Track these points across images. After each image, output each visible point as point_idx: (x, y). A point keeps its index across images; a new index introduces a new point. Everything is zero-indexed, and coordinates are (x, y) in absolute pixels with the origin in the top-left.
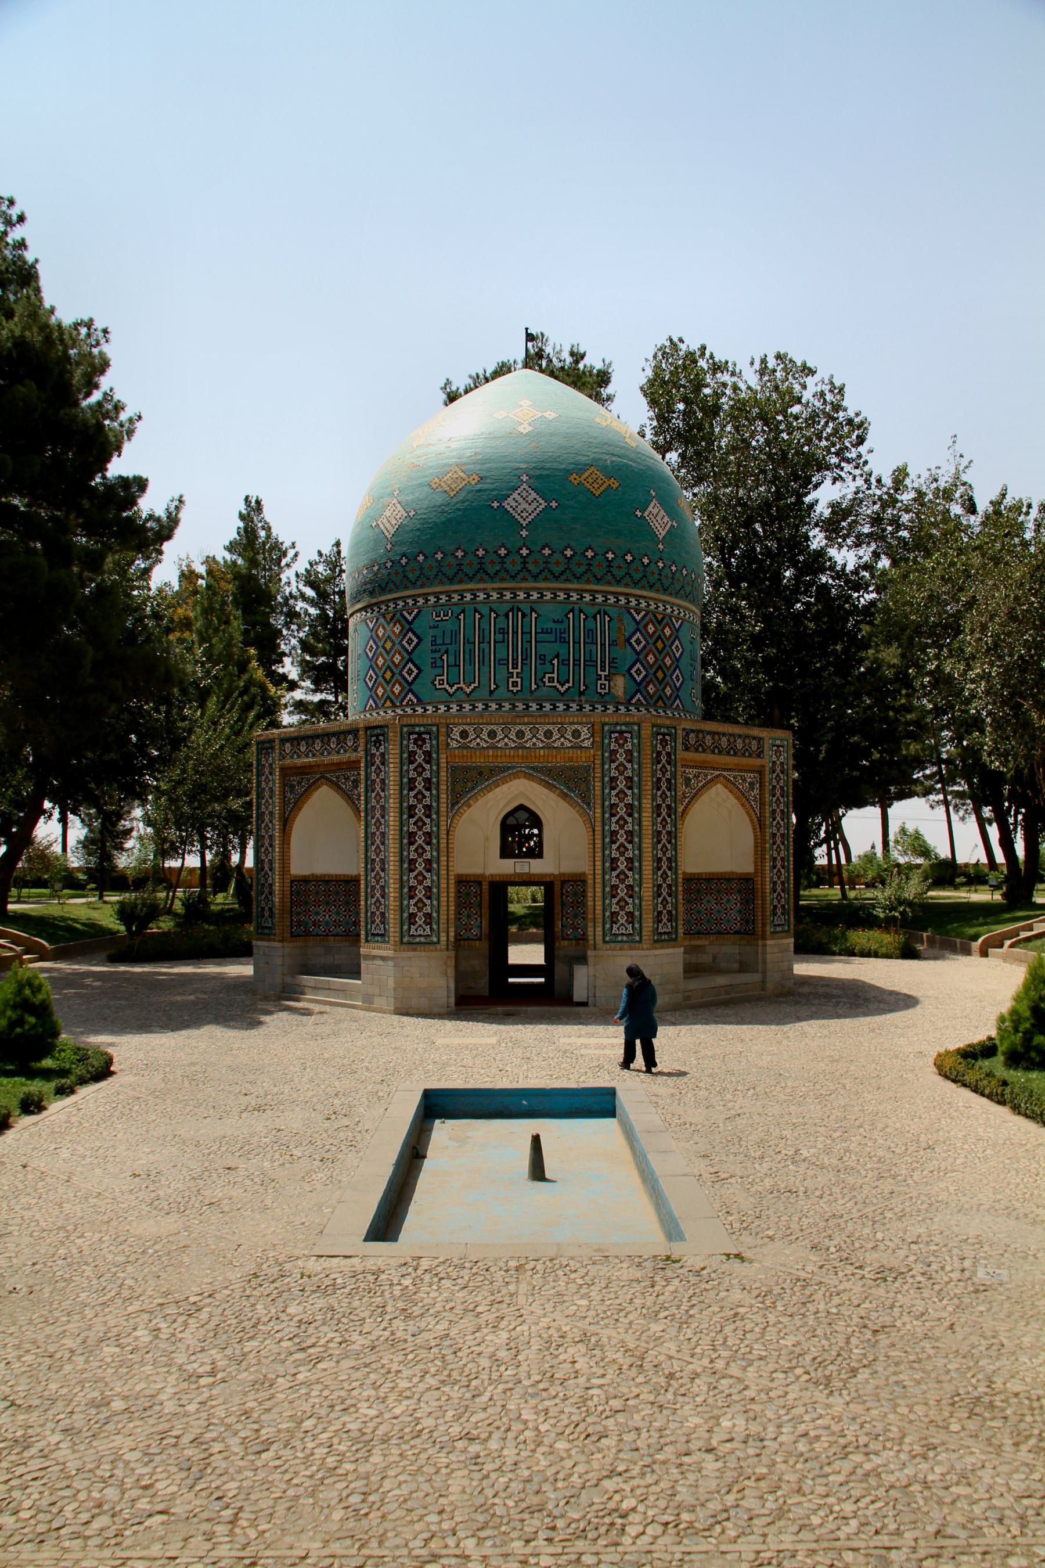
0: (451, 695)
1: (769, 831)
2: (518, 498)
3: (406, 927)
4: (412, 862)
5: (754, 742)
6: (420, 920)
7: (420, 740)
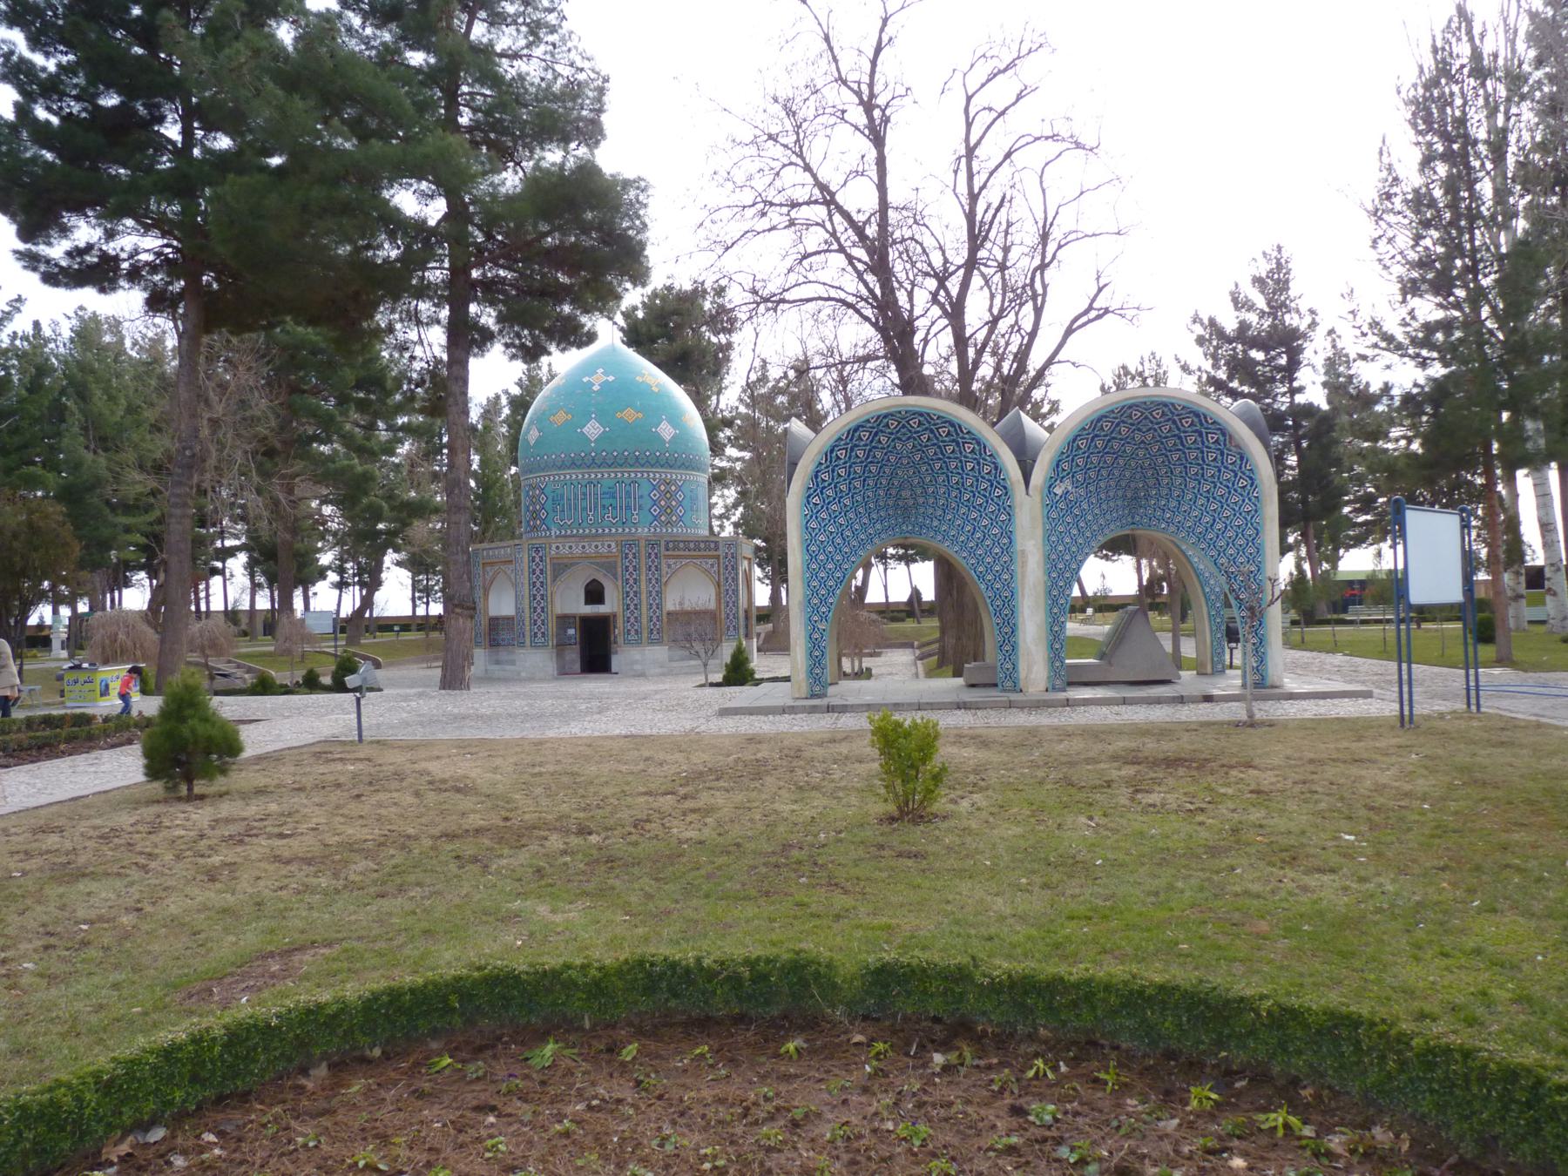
7: (537, 551)
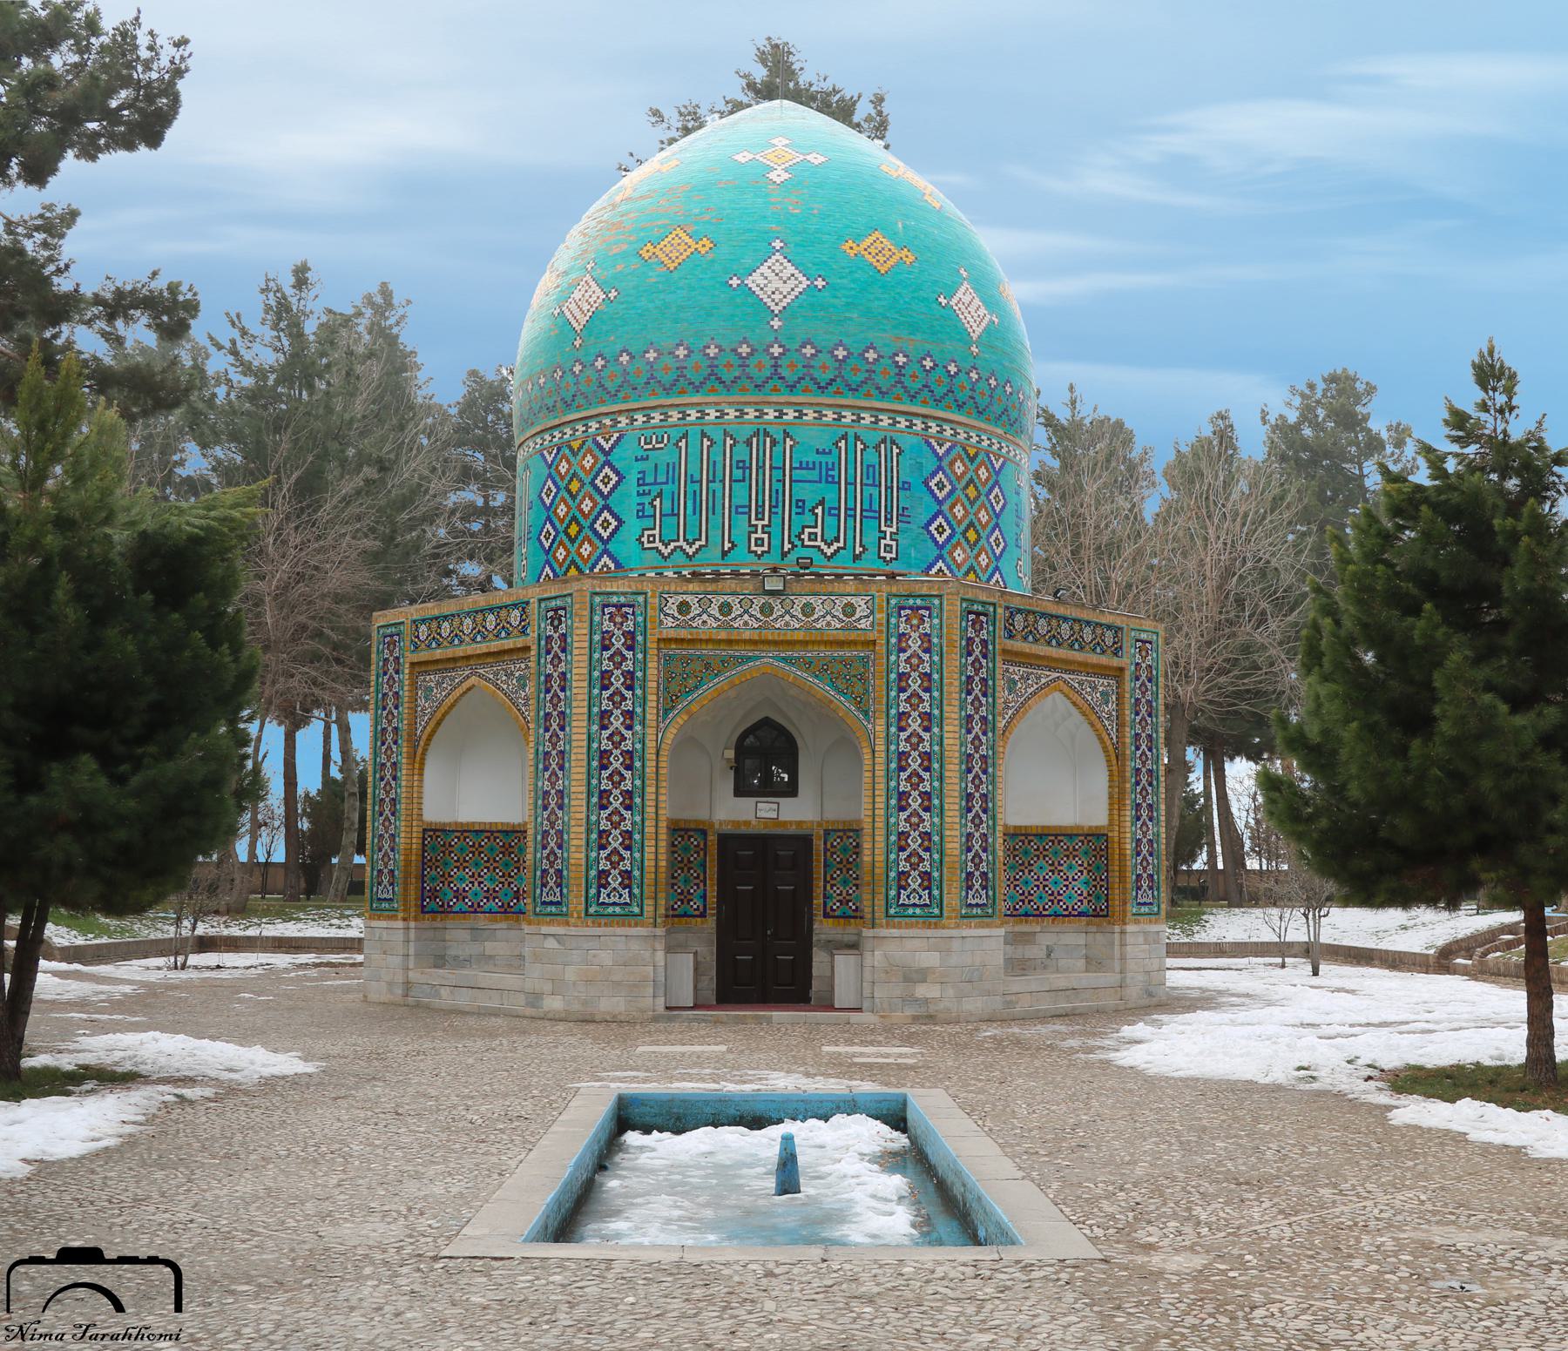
0: (665, 558)
1: (1130, 765)
2: (768, 273)
3: (593, 891)
4: (604, 794)
5: (1109, 634)
6: (615, 881)
